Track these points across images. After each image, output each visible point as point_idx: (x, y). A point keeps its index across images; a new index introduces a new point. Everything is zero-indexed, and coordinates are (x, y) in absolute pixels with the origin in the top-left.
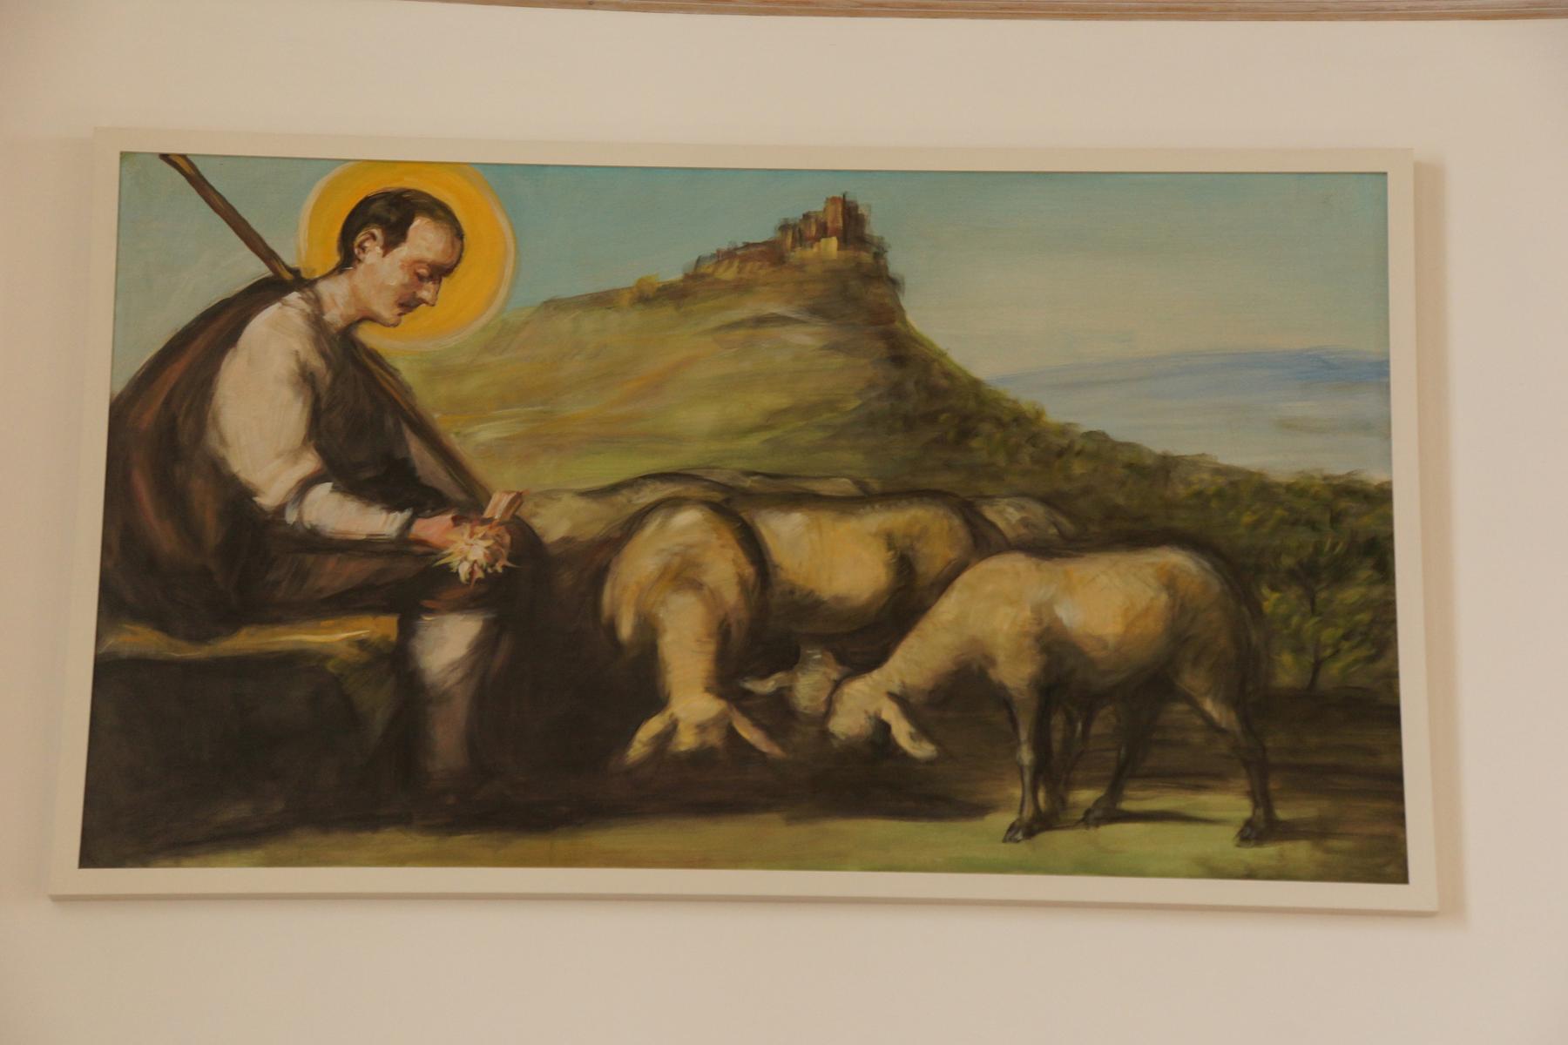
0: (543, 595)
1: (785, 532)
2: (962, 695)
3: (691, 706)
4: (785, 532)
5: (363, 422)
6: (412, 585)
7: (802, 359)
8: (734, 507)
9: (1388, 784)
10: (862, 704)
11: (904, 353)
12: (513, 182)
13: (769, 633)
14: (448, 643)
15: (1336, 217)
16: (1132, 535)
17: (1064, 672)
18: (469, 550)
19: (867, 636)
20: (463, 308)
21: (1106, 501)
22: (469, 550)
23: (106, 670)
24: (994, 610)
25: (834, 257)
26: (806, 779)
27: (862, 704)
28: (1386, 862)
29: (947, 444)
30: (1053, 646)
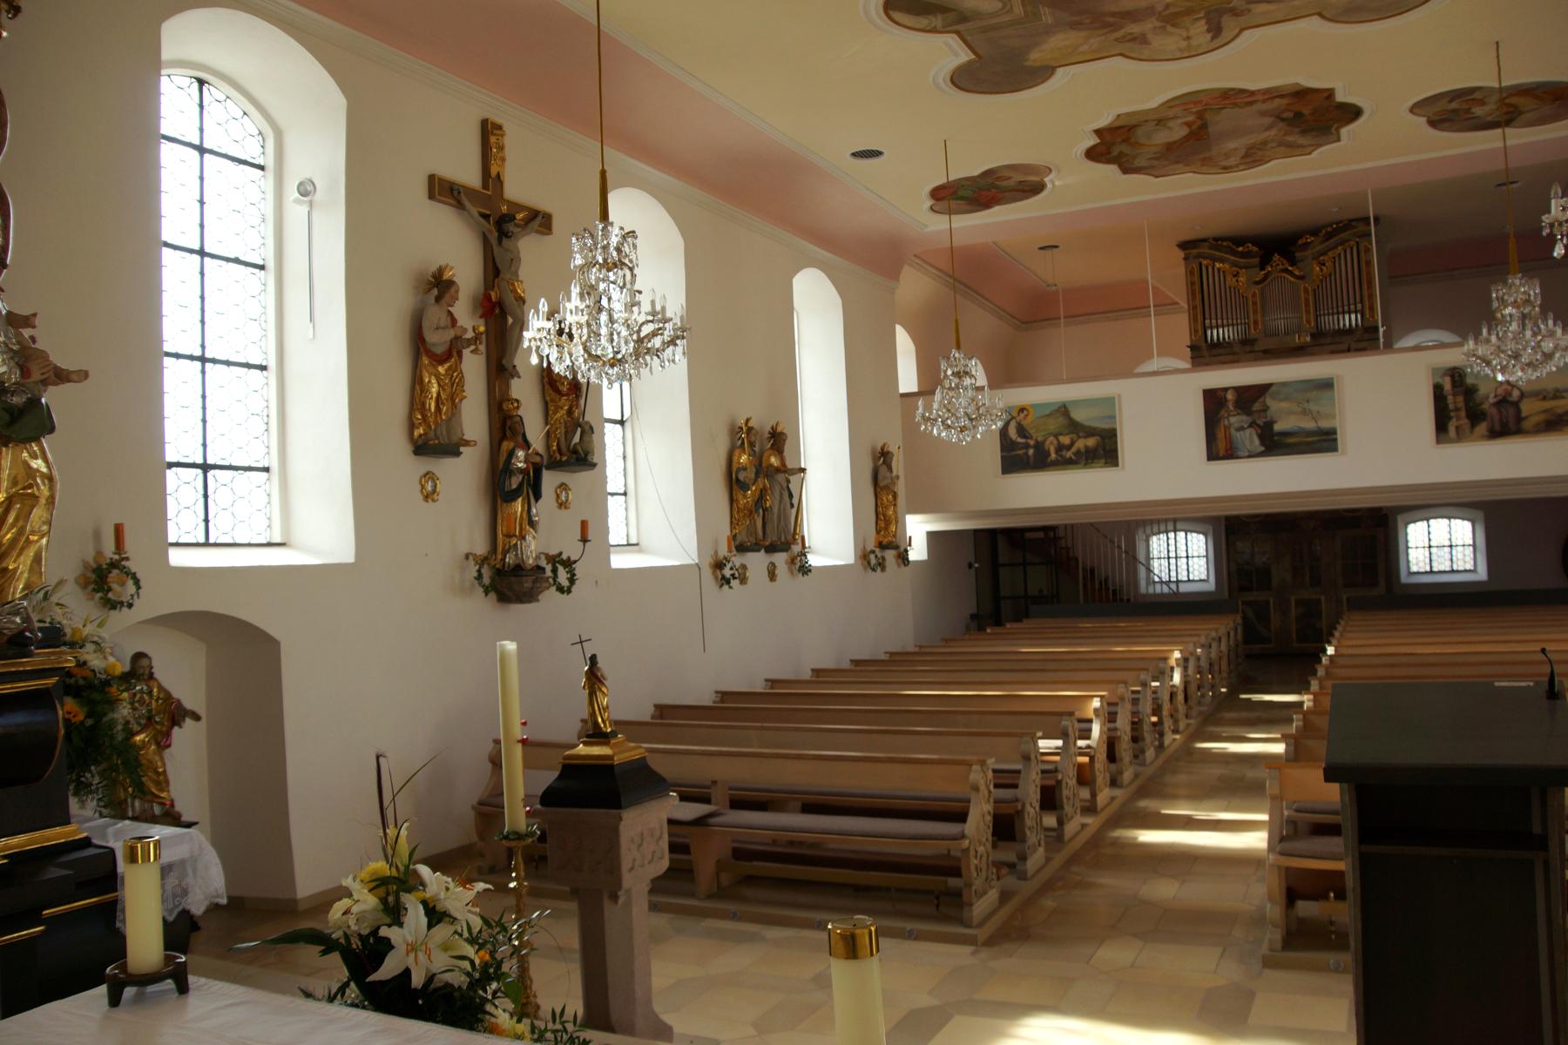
0: (1039, 446)
1: (1061, 438)
2: (1078, 453)
3: (1053, 456)
4: (1061, 438)
5: (1022, 431)
6: (1027, 446)
7: (1061, 420)
8: (1056, 436)
9: (1117, 457)
10: (1069, 454)
11: (1071, 419)
12: (1034, 406)
13: (1060, 448)
14: (1031, 452)
15: (1110, 402)
16: (1093, 435)
17: (1088, 450)
19: (1069, 448)
20: (1030, 418)
21: (1091, 432)
24: (1081, 444)
25: (1063, 410)
26: (1064, 463)
27: (1069, 454)
28: (1116, 465)
29: (1075, 428)
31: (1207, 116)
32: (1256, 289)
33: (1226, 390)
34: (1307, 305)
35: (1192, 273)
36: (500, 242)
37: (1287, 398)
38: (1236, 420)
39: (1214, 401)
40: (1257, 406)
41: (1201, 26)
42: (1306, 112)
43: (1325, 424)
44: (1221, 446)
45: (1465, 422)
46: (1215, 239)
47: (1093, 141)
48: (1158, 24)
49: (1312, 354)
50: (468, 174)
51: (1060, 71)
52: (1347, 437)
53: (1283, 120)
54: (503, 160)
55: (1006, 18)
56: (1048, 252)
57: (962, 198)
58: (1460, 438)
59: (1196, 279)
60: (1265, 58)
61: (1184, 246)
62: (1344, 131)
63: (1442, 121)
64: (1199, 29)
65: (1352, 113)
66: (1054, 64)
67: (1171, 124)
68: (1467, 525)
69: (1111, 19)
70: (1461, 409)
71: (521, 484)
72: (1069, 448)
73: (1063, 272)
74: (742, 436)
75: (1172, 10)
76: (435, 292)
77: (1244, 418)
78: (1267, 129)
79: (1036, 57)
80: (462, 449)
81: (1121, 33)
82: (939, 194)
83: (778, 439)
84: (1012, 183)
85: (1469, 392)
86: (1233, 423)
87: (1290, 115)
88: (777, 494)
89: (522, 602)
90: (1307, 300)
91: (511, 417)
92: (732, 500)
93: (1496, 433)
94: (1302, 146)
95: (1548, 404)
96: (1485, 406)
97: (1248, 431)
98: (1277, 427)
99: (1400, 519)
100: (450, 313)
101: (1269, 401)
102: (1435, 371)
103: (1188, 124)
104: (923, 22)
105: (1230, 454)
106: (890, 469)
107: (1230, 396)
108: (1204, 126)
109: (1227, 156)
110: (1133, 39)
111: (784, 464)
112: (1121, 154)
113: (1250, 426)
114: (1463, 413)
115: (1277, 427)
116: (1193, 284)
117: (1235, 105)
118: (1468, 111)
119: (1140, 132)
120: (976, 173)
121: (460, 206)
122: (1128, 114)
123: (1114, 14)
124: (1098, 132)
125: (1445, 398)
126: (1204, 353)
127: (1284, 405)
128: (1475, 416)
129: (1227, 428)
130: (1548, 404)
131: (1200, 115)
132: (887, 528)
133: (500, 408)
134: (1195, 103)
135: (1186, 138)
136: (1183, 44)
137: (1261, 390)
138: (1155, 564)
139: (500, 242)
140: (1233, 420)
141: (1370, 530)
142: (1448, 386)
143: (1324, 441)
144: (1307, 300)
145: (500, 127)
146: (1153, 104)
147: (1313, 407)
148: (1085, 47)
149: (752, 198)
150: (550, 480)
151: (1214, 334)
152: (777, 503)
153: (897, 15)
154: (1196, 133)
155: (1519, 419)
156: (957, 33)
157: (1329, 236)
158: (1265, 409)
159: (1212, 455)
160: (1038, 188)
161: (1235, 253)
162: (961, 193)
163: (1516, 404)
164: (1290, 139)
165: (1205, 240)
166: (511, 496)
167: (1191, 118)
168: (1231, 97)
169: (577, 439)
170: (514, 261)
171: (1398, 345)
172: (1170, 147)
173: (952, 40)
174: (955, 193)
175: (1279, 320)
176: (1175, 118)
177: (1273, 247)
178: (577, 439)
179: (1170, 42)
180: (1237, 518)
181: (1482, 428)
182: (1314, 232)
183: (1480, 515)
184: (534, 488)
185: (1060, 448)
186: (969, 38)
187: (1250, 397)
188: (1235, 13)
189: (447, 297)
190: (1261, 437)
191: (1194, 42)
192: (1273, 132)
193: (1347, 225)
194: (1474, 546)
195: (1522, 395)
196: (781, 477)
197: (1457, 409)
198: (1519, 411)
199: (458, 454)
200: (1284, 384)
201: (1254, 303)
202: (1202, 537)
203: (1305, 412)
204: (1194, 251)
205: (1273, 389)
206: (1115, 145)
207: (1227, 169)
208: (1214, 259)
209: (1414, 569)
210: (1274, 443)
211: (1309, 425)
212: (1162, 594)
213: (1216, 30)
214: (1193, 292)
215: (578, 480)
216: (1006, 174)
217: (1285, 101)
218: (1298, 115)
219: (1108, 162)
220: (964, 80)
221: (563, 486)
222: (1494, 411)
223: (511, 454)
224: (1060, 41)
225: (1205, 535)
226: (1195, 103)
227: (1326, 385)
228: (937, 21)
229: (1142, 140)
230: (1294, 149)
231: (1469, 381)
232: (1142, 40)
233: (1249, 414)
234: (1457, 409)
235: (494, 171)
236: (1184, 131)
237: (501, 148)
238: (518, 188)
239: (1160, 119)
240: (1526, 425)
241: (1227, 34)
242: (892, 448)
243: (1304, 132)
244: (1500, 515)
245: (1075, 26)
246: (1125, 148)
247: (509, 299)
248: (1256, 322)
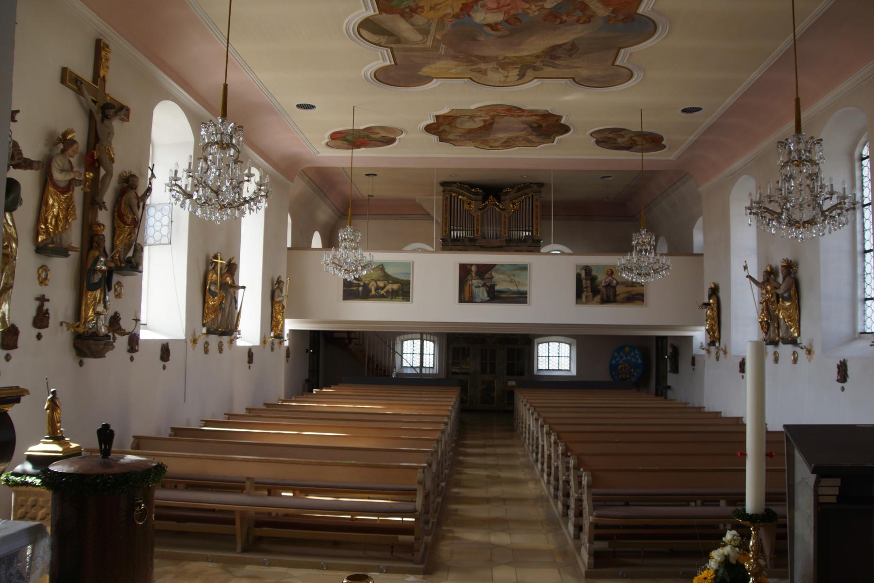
0: (366, 286)
2: (388, 292)
3: (373, 292)
7: (380, 273)
8: (376, 281)
11: (385, 273)
13: (378, 288)
14: (361, 289)
18: (362, 284)
19: (383, 288)
21: (395, 281)
22: (362, 284)
23: (344, 290)
24: (390, 287)
25: (381, 267)
26: (379, 297)
27: (382, 292)
28: (409, 300)
29: (387, 277)
30: (393, 289)
31: (496, 119)
32: (480, 213)
33: (472, 265)
34: (505, 224)
35: (446, 199)
36: (103, 121)
37: (503, 273)
38: (475, 282)
39: (465, 270)
40: (487, 275)
41: (516, 72)
42: (544, 125)
43: (521, 289)
44: (467, 295)
45: (590, 294)
46: (461, 183)
47: (431, 121)
48: (495, 66)
49: (506, 251)
50: (86, 73)
51: (435, 80)
52: (533, 297)
53: (531, 127)
54: (108, 67)
55: (422, 46)
56: (371, 178)
57: (346, 140)
58: (587, 302)
59: (448, 203)
60: (537, 95)
61: (444, 184)
62: (557, 138)
63: (604, 142)
64: (514, 73)
65: (565, 129)
66: (433, 76)
67: (476, 119)
68: (567, 346)
69: (474, 59)
70: (589, 287)
71: (101, 280)
72: (383, 288)
73: (364, 189)
74: (210, 263)
75: (507, 60)
76: (61, 146)
77: (480, 281)
78: (522, 130)
79: (426, 71)
80: (70, 253)
81: (474, 67)
82: (335, 136)
83: (232, 268)
84: (378, 136)
85: (593, 279)
86: (474, 284)
87: (535, 125)
88: (229, 300)
89: (95, 357)
90: (505, 222)
91: (97, 235)
92: (205, 302)
93: (604, 301)
94: (534, 142)
95: (629, 289)
96: (600, 287)
98: (497, 288)
99: (536, 341)
100: (70, 162)
101: (494, 274)
102: (577, 266)
103: (485, 121)
104: (375, 38)
105: (471, 300)
106: (281, 291)
107: (473, 269)
108: (492, 124)
109: (496, 141)
110: (479, 71)
111: (233, 282)
112: (444, 131)
114: (589, 289)
115: (497, 288)
116: (446, 205)
117: (512, 116)
118: (615, 140)
119: (459, 120)
120: (362, 127)
121: (79, 92)
122: (457, 110)
123: (477, 56)
124: (437, 117)
125: (581, 281)
126: (449, 244)
127: (501, 276)
128: (595, 291)
129: (470, 286)
130: (629, 289)
131: (493, 118)
132: (277, 326)
133: (91, 227)
134: (494, 111)
135: (481, 128)
136: (503, 79)
137: (491, 267)
138: (404, 356)
139: (103, 121)
140: (474, 281)
141: (519, 346)
142: (583, 275)
143: (520, 297)
144: (505, 222)
145: (108, 47)
146: (473, 107)
147: (516, 279)
148: (453, 71)
149: (227, 122)
150: (116, 278)
151: (454, 234)
152: (228, 305)
153: (364, 32)
154: (484, 128)
155: (615, 295)
156: (391, 49)
157: (519, 190)
158: (492, 278)
159: (462, 300)
160: (391, 141)
161: (470, 192)
162: (349, 138)
163: (614, 288)
164: (530, 137)
165: (455, 183)
166: (93, 287)
167: (487, 118)
168: (513, 111)
169: (130, 254)
170: (110, 134)
171: (542, 250)
172: (470, 131)
173: (387, 52)
174: (344, 137)
175: (491, 231)
176: (480, 116)
177: (490, 191)
178: (130, 254)
179: (495, 76)
180: (454, 334)
181: (598, 298)
182: (512, 186)
183: (574, 341)
184: (107, 283)
185: (378, 288)
186: (395, 53)
187: (484, 270)
188: (535, 69)
189: (70, 151)
190: (487, 292)
191: (509, 79)
192: (524, 133)
193: (528, 186)
194: (570, 357)
195: (617, 283)
196: (232, 290)
197: (587, 287)
198: (615, 291)
199: (67, 255)
200: (502, 265)
201: (478, 220)
202: (432, 343)
203: (512, 281)
204: (449, 188)
205: (497, 267)
206: (442, 128)
207: (492, 147)
208: (459, 194)
209: (540, 368)
210: (495, 296)
211: (513, 288)
212: (429, 374)
213: (521, 76)
214: (446, 210)
215: (127, 280)
216: (377, 131)
217: (537, 118)
218: (540, 126)
219: (434, 134)
220: (383, 77)
221: (119, 283)
222: (604, 290)
223: (96, 260)
224: (442, 64)
225: (434, 342)
226: (494, 111)
227: (524, 268)
228: (383, 40)
229: (459, 126)
230: (529, 143)
231: (594, 273)
232: (484, 73)
233: (482, 279)
234: (587, 287)
235: (102, 73)
236: (482, 124)
237: (107, 60)
238: (117, 88)
239: (471, 115)
240: (618, 298)
241: (526, 79)
242: (283, 279)
243: (538, 135)
244: (585, 341)
245: (455, 58)
246: (447, 128)
247: (105, 159)
248: (478, 230)
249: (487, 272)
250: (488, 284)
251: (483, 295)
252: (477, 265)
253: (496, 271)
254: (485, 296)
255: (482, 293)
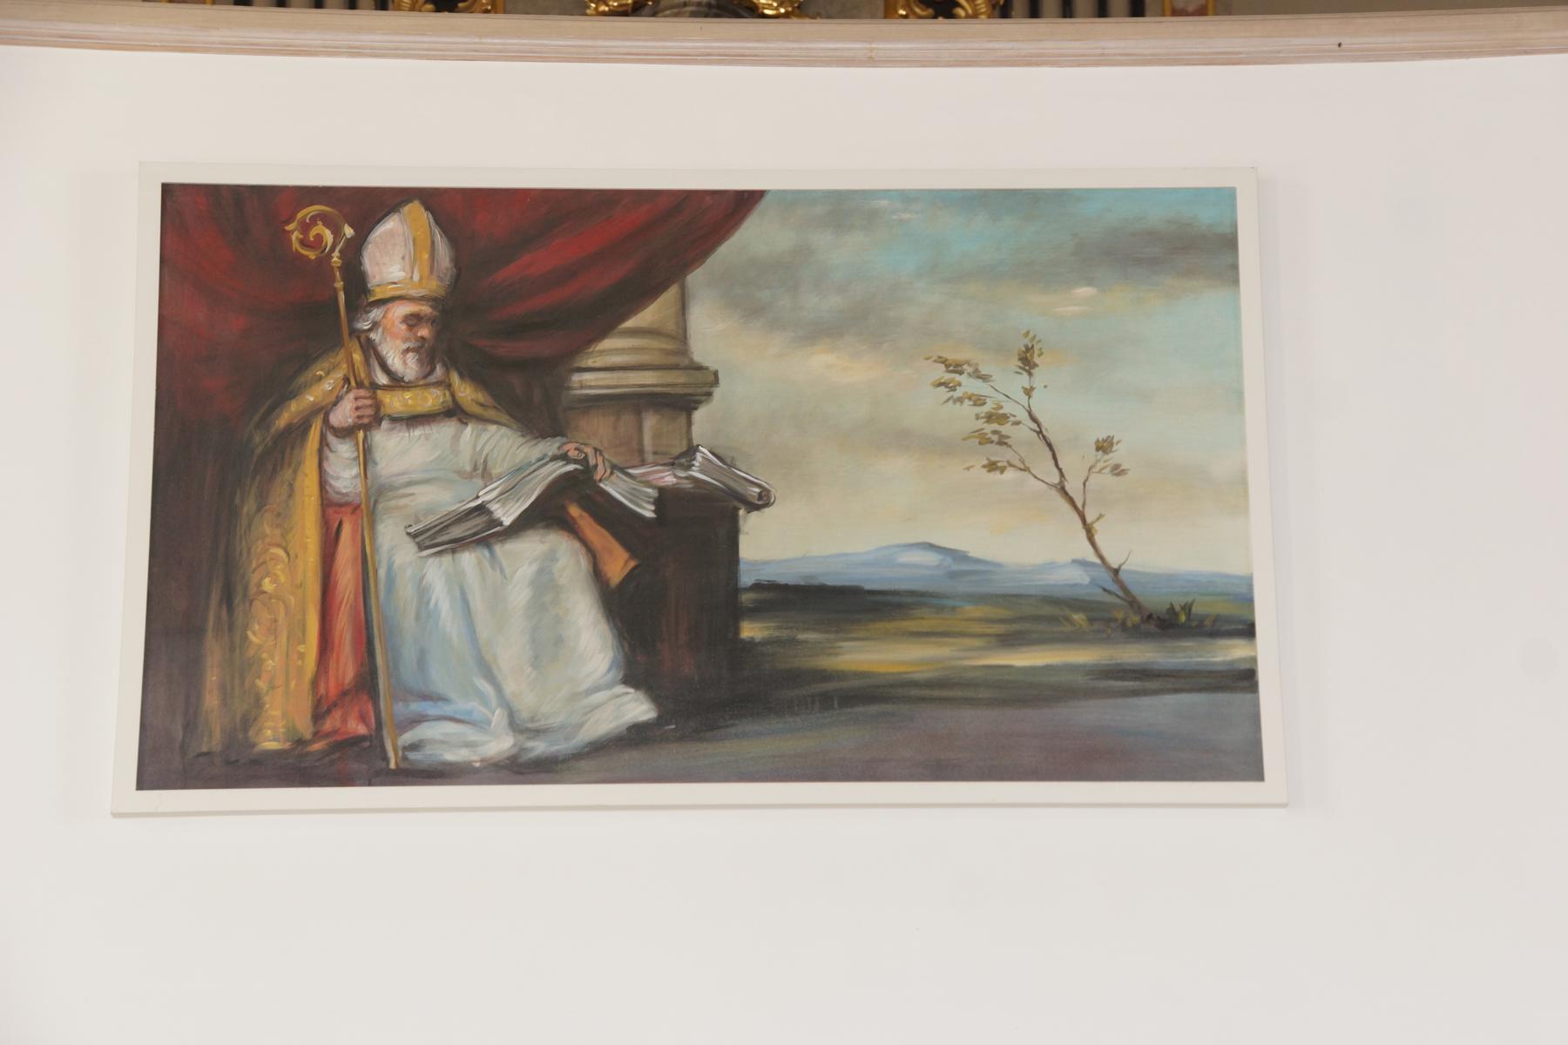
33: (366, 207)
37: (862, 322)
39: (250, 290)
40: (611, 362)
43: (1158, 550)
97: (529, 551)
98: (769, 545)
101: (712, 332)
105: (355, 741)
107: (397, 260)
113: (546, 514)
115: (769, 545)
127: (835, 370)
137: (668, 236)
140: (402, 452)
147: (1063, 403)
187: (555, 287)
190: (632, 613)
200: (844, 210)
203: (993, 438)
205: (752, 238)
211: (1030, 544)
227: (1184, 245)
233: (534, 401)
249: (605, 314)
250: (632, 490)
251: (548, 646)
252: (453, 210)
253: (750, 303)
254: (587, 675)
255: (528, 627)
